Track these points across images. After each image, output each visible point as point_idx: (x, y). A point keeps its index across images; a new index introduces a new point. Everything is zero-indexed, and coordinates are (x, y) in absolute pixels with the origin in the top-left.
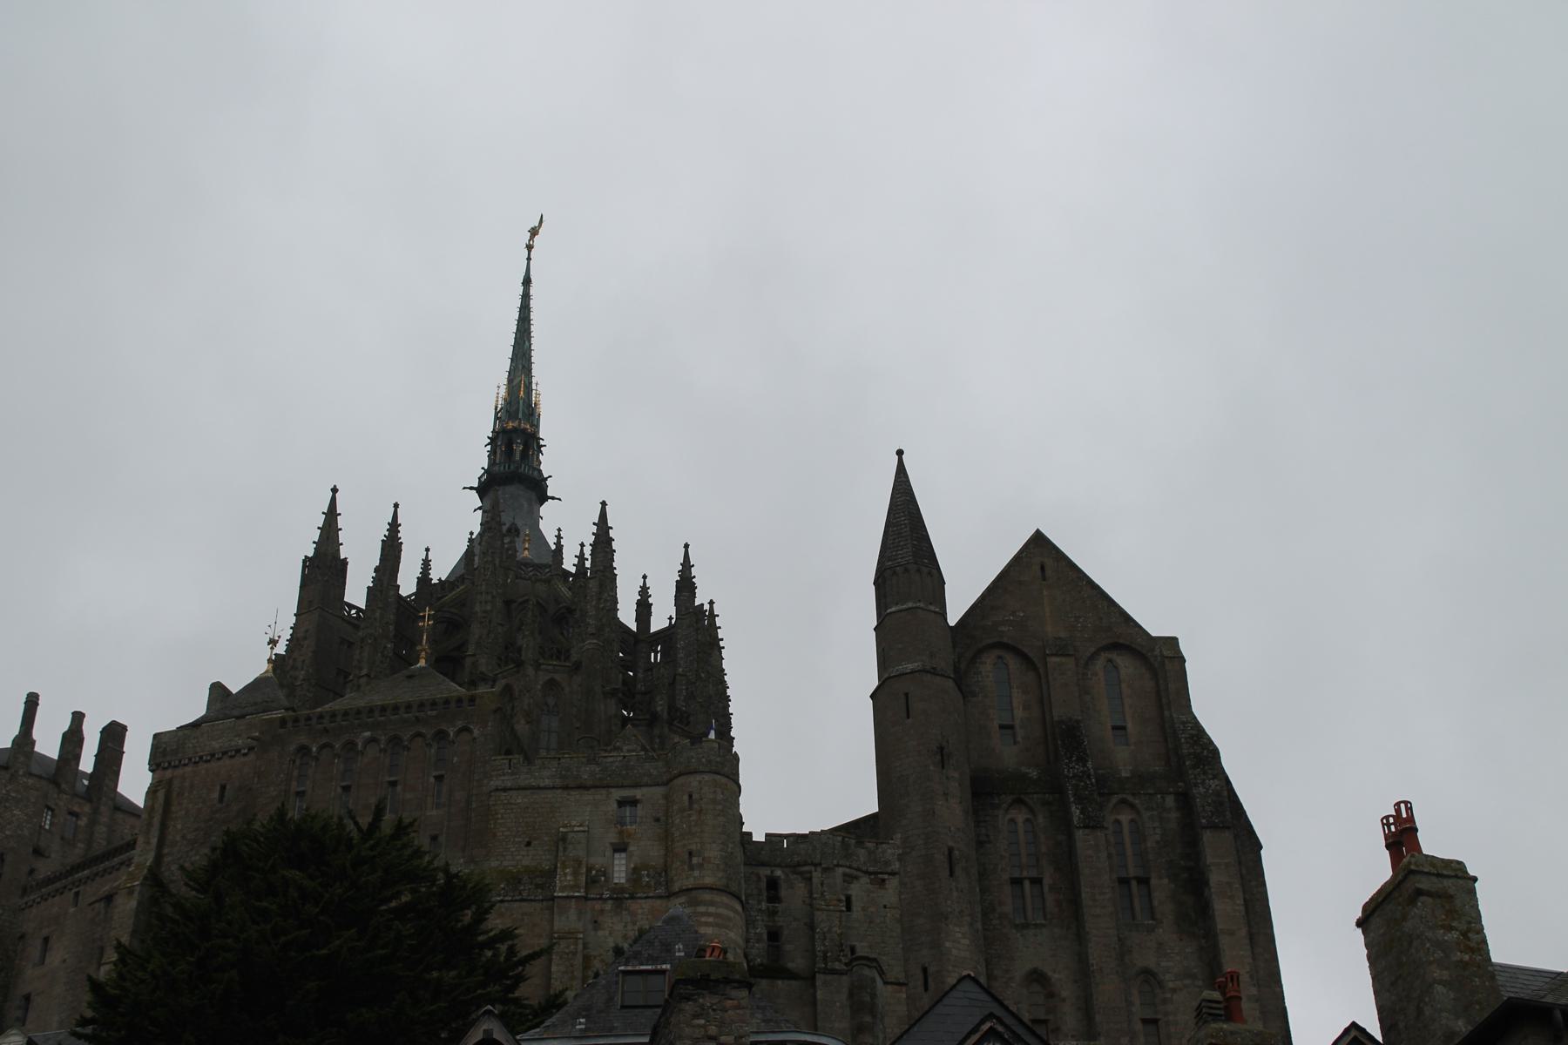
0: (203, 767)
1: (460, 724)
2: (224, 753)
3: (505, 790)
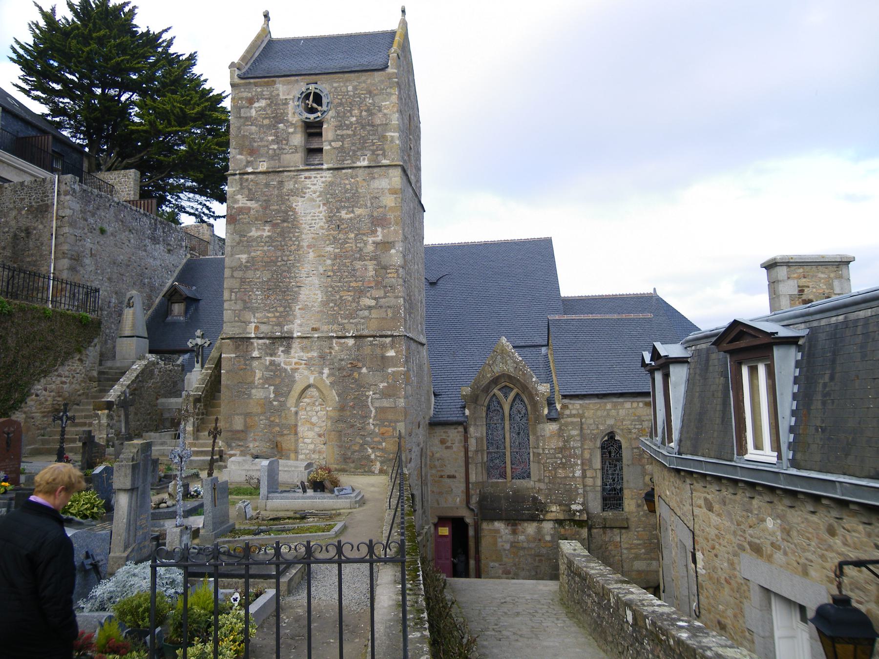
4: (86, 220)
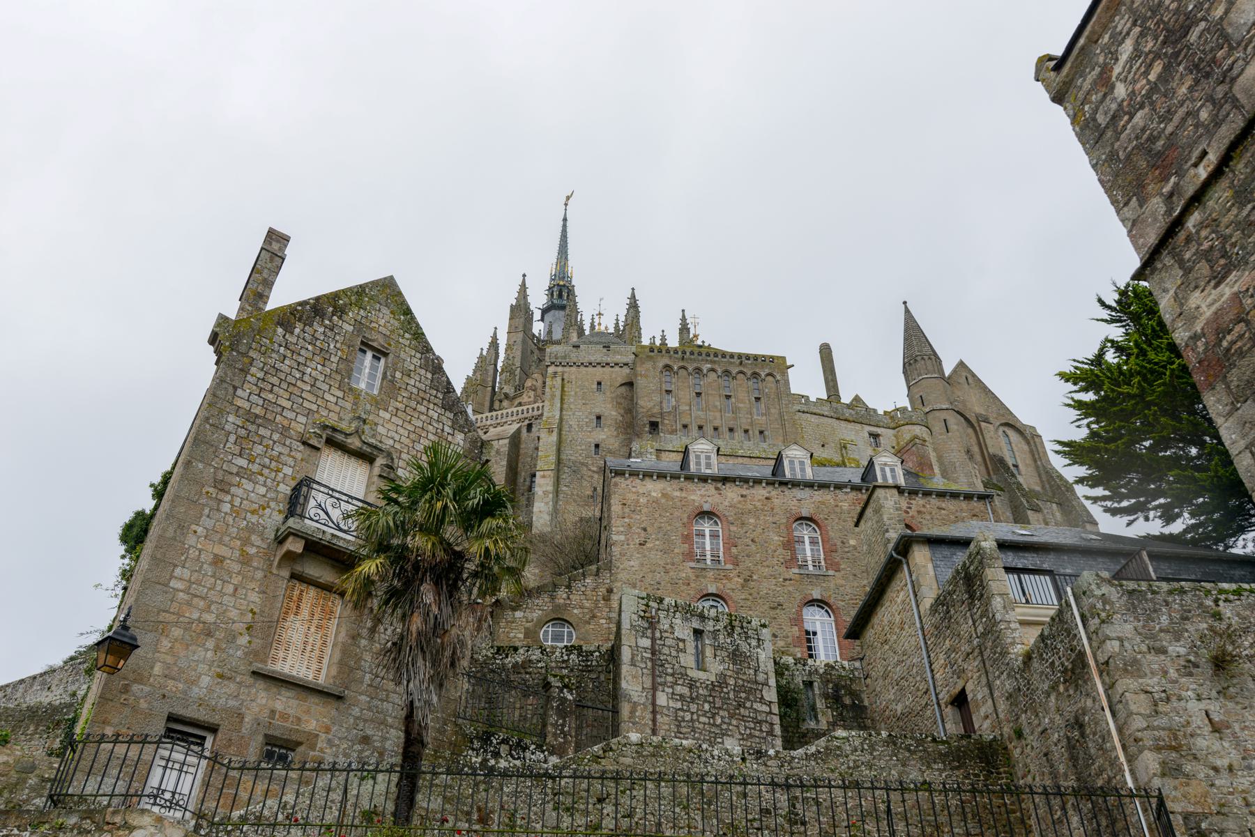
1: (767, 371)
3: (804, 412)
4: (1163, 651)
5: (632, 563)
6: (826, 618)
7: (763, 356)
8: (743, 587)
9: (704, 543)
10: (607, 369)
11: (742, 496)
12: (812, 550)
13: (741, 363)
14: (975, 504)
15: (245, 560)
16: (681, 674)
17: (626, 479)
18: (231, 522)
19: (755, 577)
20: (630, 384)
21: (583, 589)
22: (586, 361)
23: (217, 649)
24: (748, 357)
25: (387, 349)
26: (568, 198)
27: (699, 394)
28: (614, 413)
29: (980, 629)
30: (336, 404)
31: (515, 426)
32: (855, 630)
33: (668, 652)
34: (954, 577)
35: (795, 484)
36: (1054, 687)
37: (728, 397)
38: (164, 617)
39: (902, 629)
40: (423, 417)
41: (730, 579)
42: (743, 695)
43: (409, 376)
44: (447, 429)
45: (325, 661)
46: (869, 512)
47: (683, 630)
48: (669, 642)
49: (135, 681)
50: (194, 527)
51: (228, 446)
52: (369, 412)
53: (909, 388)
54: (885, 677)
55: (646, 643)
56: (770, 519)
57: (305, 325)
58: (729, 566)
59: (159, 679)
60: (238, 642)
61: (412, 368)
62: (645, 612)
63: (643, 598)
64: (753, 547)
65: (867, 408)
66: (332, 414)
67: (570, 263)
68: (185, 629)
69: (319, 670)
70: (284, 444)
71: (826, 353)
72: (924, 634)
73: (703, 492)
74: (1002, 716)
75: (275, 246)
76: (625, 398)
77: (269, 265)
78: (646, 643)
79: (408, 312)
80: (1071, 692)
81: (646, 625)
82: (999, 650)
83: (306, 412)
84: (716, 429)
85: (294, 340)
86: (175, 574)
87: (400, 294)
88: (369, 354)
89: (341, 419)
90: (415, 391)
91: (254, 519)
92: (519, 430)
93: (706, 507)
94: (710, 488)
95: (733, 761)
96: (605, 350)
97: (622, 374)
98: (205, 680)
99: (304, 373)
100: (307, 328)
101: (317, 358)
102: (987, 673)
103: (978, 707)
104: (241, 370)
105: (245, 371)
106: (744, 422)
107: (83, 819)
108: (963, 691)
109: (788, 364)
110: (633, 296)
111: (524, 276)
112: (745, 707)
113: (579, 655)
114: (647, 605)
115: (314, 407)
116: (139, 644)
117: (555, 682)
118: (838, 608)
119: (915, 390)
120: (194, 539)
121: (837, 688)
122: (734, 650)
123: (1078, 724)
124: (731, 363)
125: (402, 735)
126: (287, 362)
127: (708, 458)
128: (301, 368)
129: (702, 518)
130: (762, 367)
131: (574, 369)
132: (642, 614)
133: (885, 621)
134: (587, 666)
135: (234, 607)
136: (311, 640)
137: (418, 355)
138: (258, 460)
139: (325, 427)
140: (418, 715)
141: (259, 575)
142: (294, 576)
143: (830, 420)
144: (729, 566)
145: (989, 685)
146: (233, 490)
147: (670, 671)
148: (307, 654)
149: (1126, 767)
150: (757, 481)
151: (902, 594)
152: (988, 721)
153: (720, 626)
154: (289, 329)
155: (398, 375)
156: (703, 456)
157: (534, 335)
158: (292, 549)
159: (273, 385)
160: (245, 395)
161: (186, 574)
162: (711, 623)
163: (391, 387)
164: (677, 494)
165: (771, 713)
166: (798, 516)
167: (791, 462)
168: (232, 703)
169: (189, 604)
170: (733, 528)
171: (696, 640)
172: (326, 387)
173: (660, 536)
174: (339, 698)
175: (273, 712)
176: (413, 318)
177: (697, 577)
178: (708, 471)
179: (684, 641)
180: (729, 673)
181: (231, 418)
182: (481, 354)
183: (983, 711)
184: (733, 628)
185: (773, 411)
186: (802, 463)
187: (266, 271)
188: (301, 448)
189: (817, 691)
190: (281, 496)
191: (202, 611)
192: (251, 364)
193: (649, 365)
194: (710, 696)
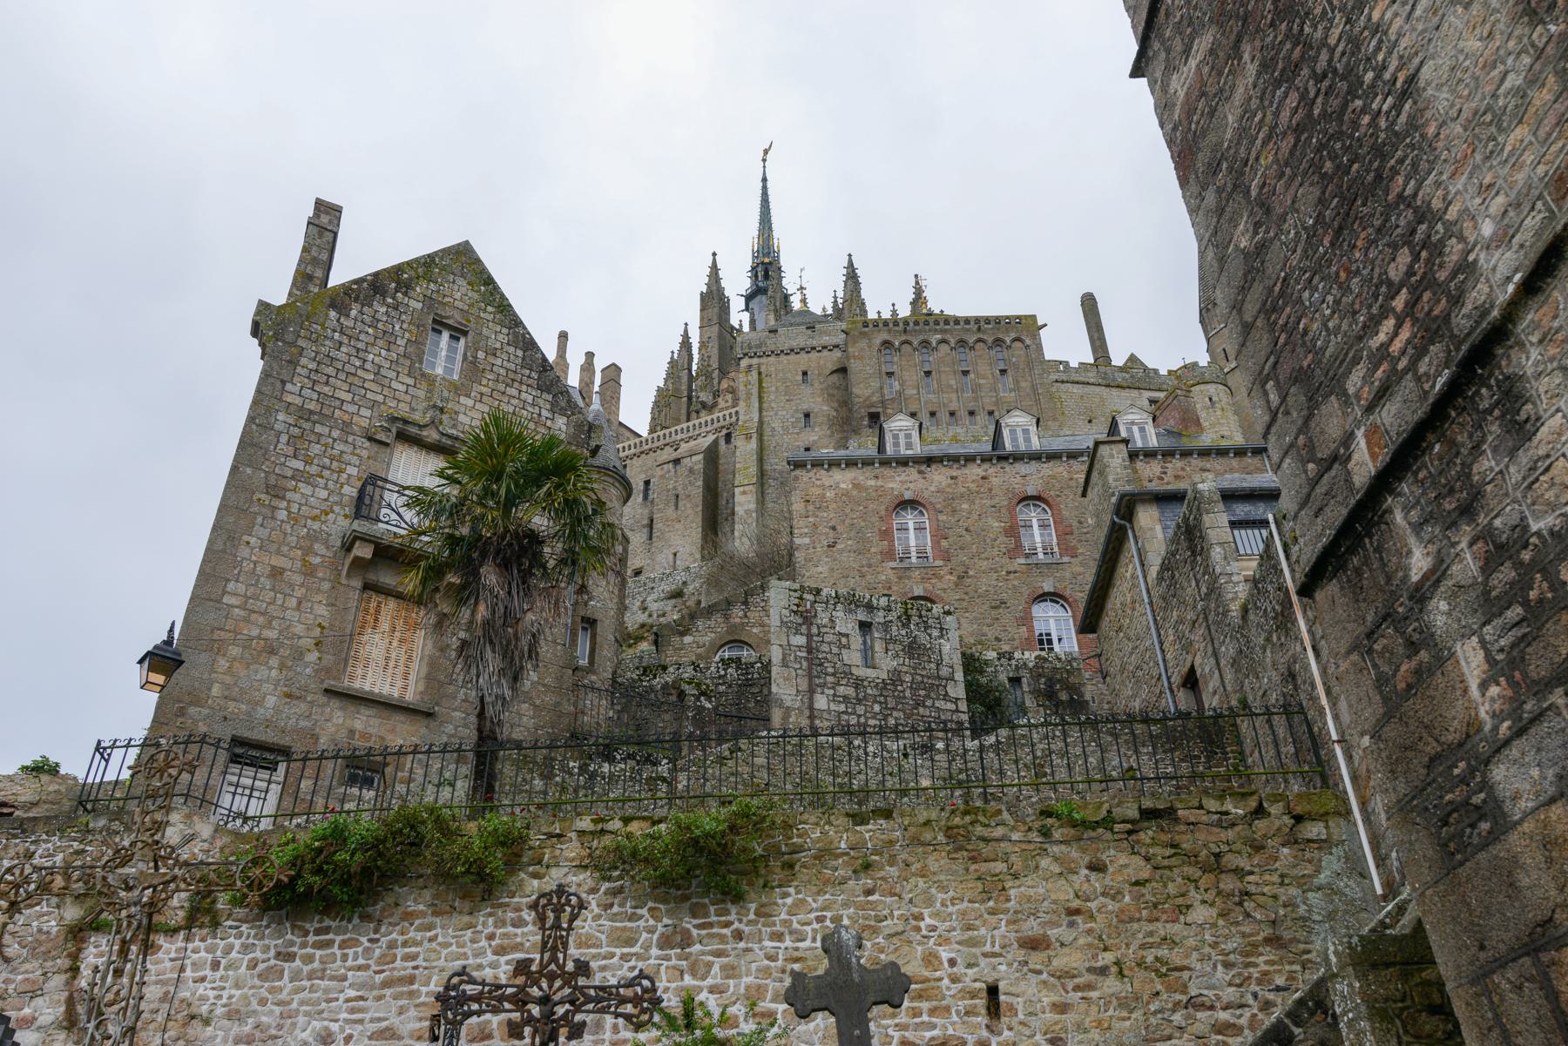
0: (783, 357)
1: (1013, 335)
2: (802, 349)
3: (1063, 382)
5: (820, 569)
6: (1062, 613)
7: (1007, 317)
8: (956, 585)
9: (907, 539)
10: (814, 355)
11: (952, 478)
12: (1042, 535)
13: (979, 329)
14: (1249, 460)
15: (309, 571)
16: (844, 672)
17: (808, 471)
18: (289, 531)
19: (971, 573)
20: (843, 371)
21: (763, 604)
22: (786, 347)
23: (282, 667)
24: (987, 320)
25: (466, 326)
26: (766, 152)
27: (928, 373)
28: (825, 408)
29: (1204, 590)
30: (406, 392)
31: (711, 438)
32: (1089, 623)
33: (827, 650)
34: (1176, 534)
35: (1017, 457)
36: (1268, 640)
37: (965, 373)
38: (217, 635)
39: (1134, 609)
40: (515, 402)
41: (940, 578)
42: (922, 693)
43: (495, 355)
44: (545, 413)
45: (412, 677)
46: (1095, 474)
47: (846, 623)
48: (828, 638)
49: (191, 703)
50: (246, 538)
51: (280, 446)
52: (447, 400)
53: (1208, 340)
54: (1122, 670)
55: (800, 640)
56: (988, 502)
57: (363, 305)
58: (939, 563)
59: (218, 701)
60: (307, 659)
61: (498, 345)
62: (798, 606)
63: (795, 591)
64: (968, 538)
65: (1146, 369)
66: (402, 405)
67: (776, 234)
68: (244, 647)
69: (405, 688)
70: (346, 442)
71: (1089, 305)
72: (1153, 611)
73: (903, 477)
74: (1229, 688)
75: (324, 219)
76: (838, 388)
77: (318, 242)
78: (800, 640)
79: (489, 281)
80: (1283, 639)
81: (800, 621)
82: (1221, 610)
83: (370, 404)
84: (952, 414)
85: (350, 323)
86: (228, 589)
87: (478, 261)
88: (446, 335)
89: (413, 409)
90: (503, 372)
91: (316, 526)
92: (716, 442)
93: (908, 496)
94: (912, 472)
95: (892, 757)
96: (809, 332)
97: (831, 359)
98: (271, 701)
99: (365, 361)
100: (366, 309)
101: (380, 343)
102: (1212, 640)
103: (1206, 683)
104: (289, 362)
105: (294, 363)
106: (988, 402)
107: (111, 820)
108: (1192, 667)
109: (1040, 323)
110: (851, 264)
111: (714, 254)
112: (924, 706)
113: (738, 668)
114: (801, 598)
115: (380, 398)
116: (183, 658)
117: (690, 690)
118: (1076, 601)
119: (1215, 342)
120: (248, 550)
121: (1051, 682)
122: (911, 643)
123: (1291, 676)
124: (968, 330)
125: (475, 732)
126: (344, 349)
127: (908, 436)
128: (361, 355)
129: (904, 509)
130: (1007, 331)
131: (772, 359)
132: (795, 608)
133: (1118, 602)
134: (747, 680)
135: (299, 621)
136: (393, 656)
137: (505, 331)
138: (316, 461)
139: (394, 419)
140: (490, 711)
141: (326, 586)
142: (367, 587)
143: (1098, 389)
144: (939, 563)
145: (1216, 655)
146: (289, 495)
147: (830, 670)
148: (390, 671)
149: (1328, 711)
150: (970, 459)
151: (1131, 567)
152: (1217, 697)
153: (892, 616)
154: (343, 310)
155: (481, 355)
156: (902, 435)
157: (732, 328)
158: (360, 555)
159: (329, 376)
160: (296, 389)
161: (241, 588)
162: (881, 613)
163: (473, 369)
164: (872, 482)
165: (957, 711)
166: (1022, 495)
167: (1013, 432)
168: (303, 723)
169: (247, 620)
170: (942, 517)
171: (864, 636)
172: (392, 375)
173: (852, 534)
174: (429, 715)
175: (352, 732)
176: (496, 288)
177: (900, 578)
178: (910, 452)
179: (847, 636)
180: (905, 669)
181: (281, 416)
182: (672, 358)
183: (1211, 685)
184: (909, 618)
185: (1023, 384)
186: (1026, 432)
187: (314, 248)
188: (367, 444)
189: (1026, 688)
190: (346, 499)
191: (262, 627)
192: (301, 355)
193: (863, 344)
194: (881, 695)
